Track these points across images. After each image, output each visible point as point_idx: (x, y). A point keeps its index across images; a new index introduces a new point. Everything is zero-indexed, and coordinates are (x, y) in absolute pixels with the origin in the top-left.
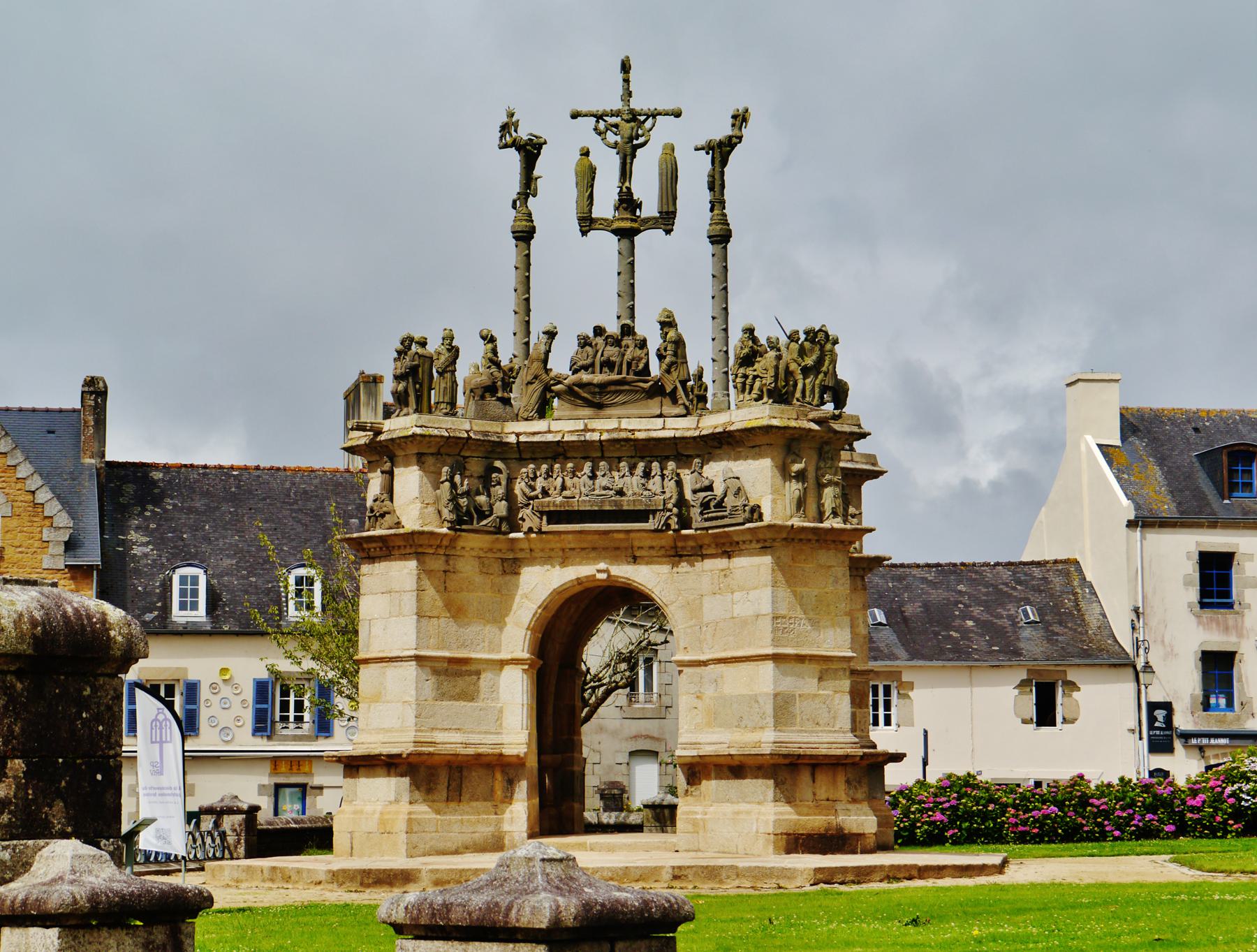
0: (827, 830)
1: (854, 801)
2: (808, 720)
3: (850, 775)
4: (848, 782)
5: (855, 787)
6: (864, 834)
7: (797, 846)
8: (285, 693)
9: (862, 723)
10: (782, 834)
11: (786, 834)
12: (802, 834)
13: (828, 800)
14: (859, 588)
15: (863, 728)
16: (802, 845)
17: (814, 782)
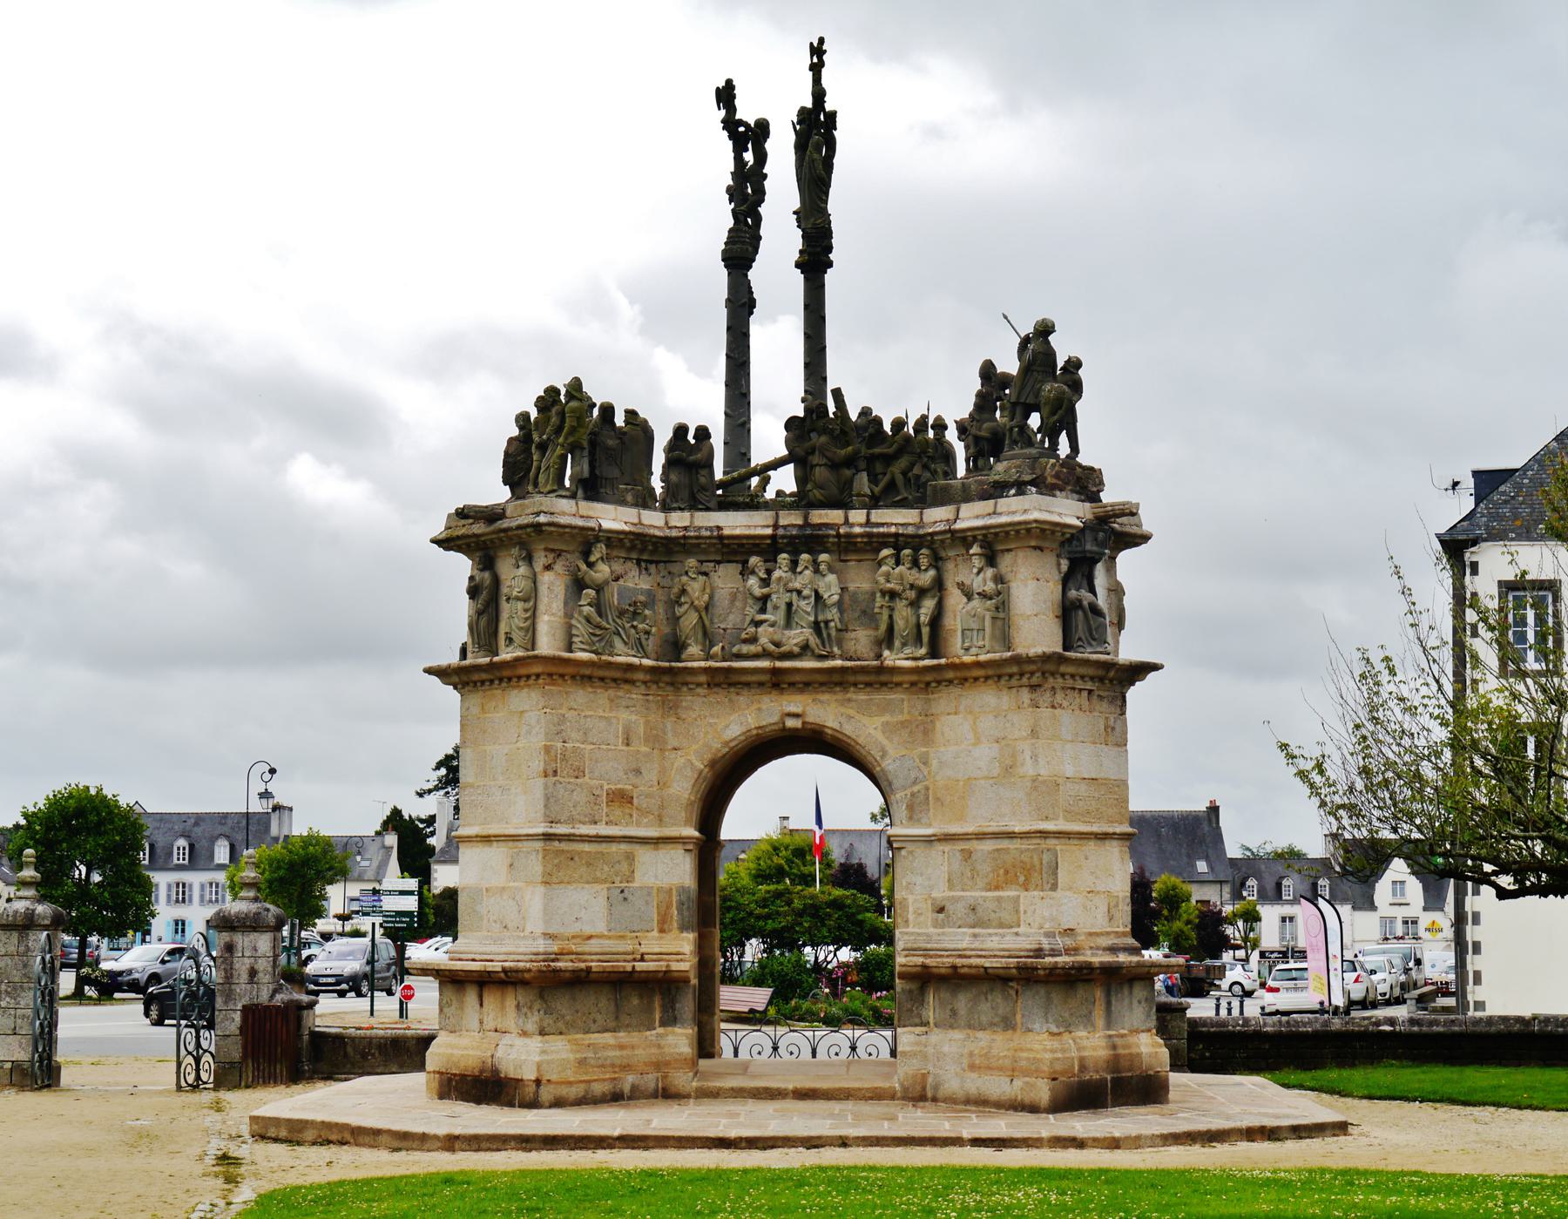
0: (482, 1071)
1: (524, 1034)
2: (495, 922)
3: (520, 998)
4: (518, 1007)
5: (526, 1014)
6: (522, 1080)
7: (450, 1090)
8: (184, 899)
9: (1029, 914)
10: (434, 1072)
11: (439, 1072)
12: (455, 1075)
13: (496, 1031)
14: (1025, 705)
15: (1030, 920)
16: (456, 1089)
17: (481, 1005)
